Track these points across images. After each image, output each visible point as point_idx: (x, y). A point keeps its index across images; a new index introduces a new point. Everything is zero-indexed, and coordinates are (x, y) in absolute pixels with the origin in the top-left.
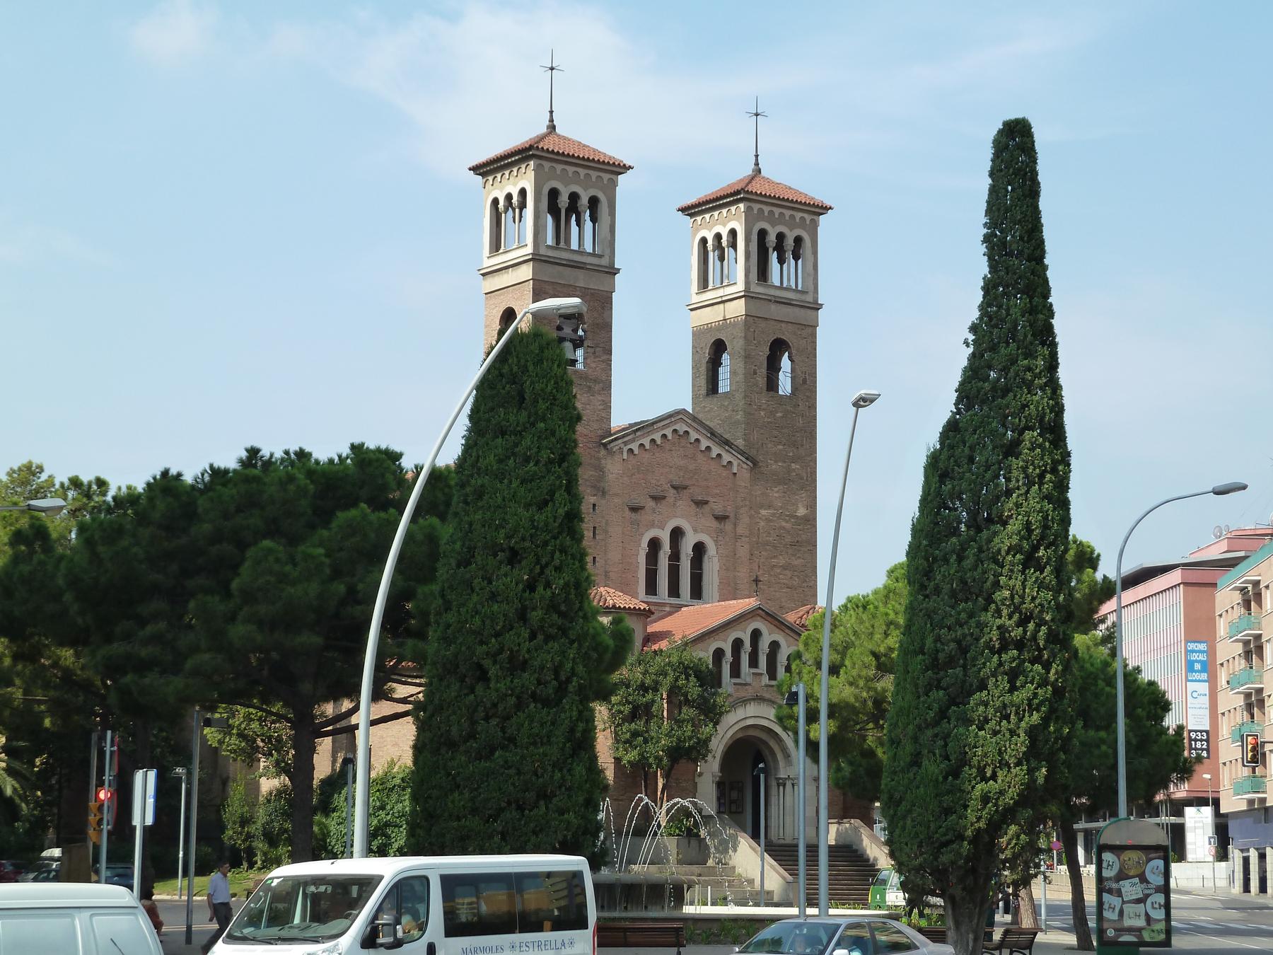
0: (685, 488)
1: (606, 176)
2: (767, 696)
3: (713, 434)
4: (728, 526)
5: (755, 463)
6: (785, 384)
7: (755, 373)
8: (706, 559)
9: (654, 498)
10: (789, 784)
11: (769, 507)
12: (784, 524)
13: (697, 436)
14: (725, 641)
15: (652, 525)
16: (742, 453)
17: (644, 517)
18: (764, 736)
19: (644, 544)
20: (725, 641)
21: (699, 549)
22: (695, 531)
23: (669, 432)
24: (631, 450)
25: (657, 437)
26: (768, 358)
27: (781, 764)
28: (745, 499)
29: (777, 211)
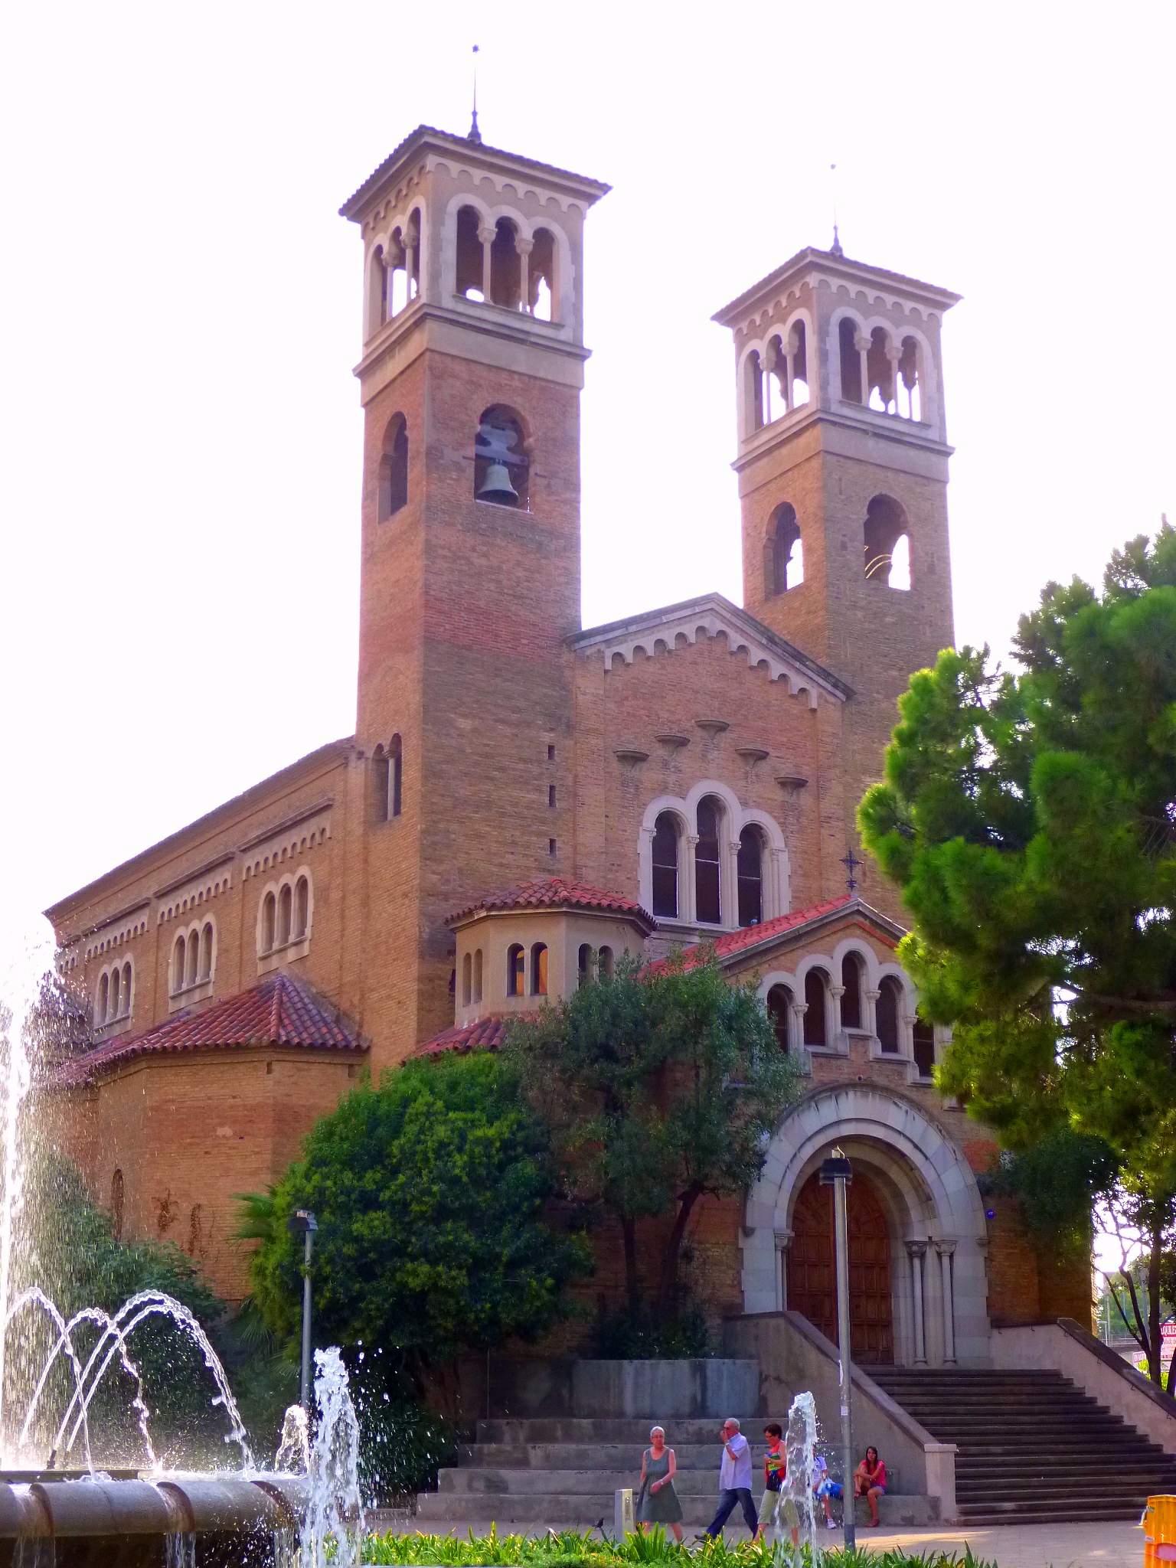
0: (722, 728)
1: (565, 201)
2: (881, 1081)
3: (772, 641)
4: (805, 799)
5: (849, 693)
6: (900, 578)
7: (844, 547)
8: (766, 856)
9: (664, 741)
10: (931, 1254)
13: (742, 641)
15: (663, 789)
16: (825, 674)
17: (648, 774)
18: (876, 1158)
20: (791, 971)
21: (752, 835)
22: (745, 804)
23: (689, 630)
24: (618, 656)
26: (865, 524)
27: (915, 1214)
29: (871, 294)
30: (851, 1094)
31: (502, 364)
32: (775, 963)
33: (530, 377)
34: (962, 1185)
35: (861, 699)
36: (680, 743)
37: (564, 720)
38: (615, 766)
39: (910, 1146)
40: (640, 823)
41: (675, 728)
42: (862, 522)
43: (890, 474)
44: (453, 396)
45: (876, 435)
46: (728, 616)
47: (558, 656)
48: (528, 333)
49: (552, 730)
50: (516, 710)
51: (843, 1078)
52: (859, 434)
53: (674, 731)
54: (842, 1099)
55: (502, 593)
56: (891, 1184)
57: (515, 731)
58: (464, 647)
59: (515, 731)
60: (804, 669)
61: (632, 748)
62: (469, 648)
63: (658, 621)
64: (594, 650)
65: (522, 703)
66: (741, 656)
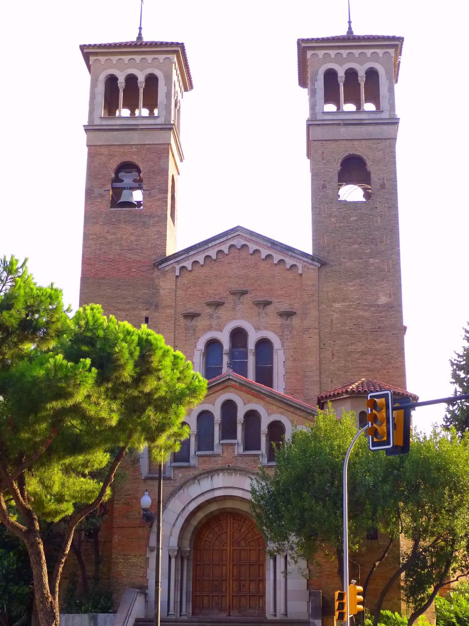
0: (244, 293)
4: (295, 321)
7: (324, 187)
9: (209, 304)
11: (344, 300)
12: (361, 313)
13: (256, 247)
17: (200, 323)
19: (201, 345)
22: (257, 329)
25: (213, 253)
28: (312, 295)
30: (221, 474)
31: (126, 143)
33: (141, 145)
35: (332, 264)
36: (218, 305)
37: (154, 304)
38: (182, 321)
40: (195, 347)
41: (218, 297)
42: (336, 172)
43: (356, 143)
44: (100, 164)
45: (345, 124)
46: (248, 236)
47: (153, 273)
48: (137, 125)
49: (147, 309)
50: (129, 303)
51: (217, 467)
52: (336, 127)
53: (217, 299)
54: (215, 478)
55: (122, 250)
57: (127, 313)
58: (102, 278)
59: (127, 313)
60: (294, 255)
61: (192, 311)
62: (103, 278)
63: (206, 247)
64: (171, 266)
65: (131, 300)
66: (257, 255)
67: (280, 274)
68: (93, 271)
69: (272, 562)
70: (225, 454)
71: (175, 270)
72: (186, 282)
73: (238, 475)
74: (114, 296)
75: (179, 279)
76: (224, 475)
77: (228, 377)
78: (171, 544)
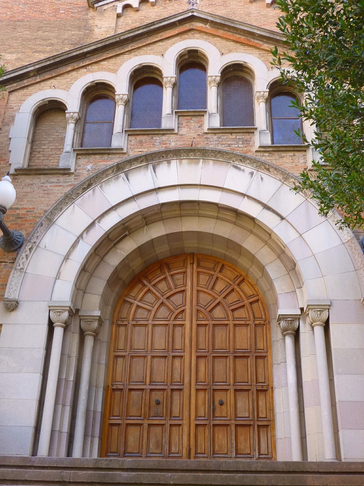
14: (115, 71)
27: (281, 286)
32: (95, 67)
34: (338, 242)
39: (260, 207)
50: (52, 45)
56: (252, 258)
58: (19, 21)
64: (111, 5)
65: (55, 41)
67: (258, 12)
68: (9, 13)
69: (289, 341)
70: (184, 131)
71: (116, 8)
72: (130, 22)
73: (211, 162)
74: (33, 37)
75: (121, 19)
76: (181, 163)
77: (190, 14)
78: (55, 298)
